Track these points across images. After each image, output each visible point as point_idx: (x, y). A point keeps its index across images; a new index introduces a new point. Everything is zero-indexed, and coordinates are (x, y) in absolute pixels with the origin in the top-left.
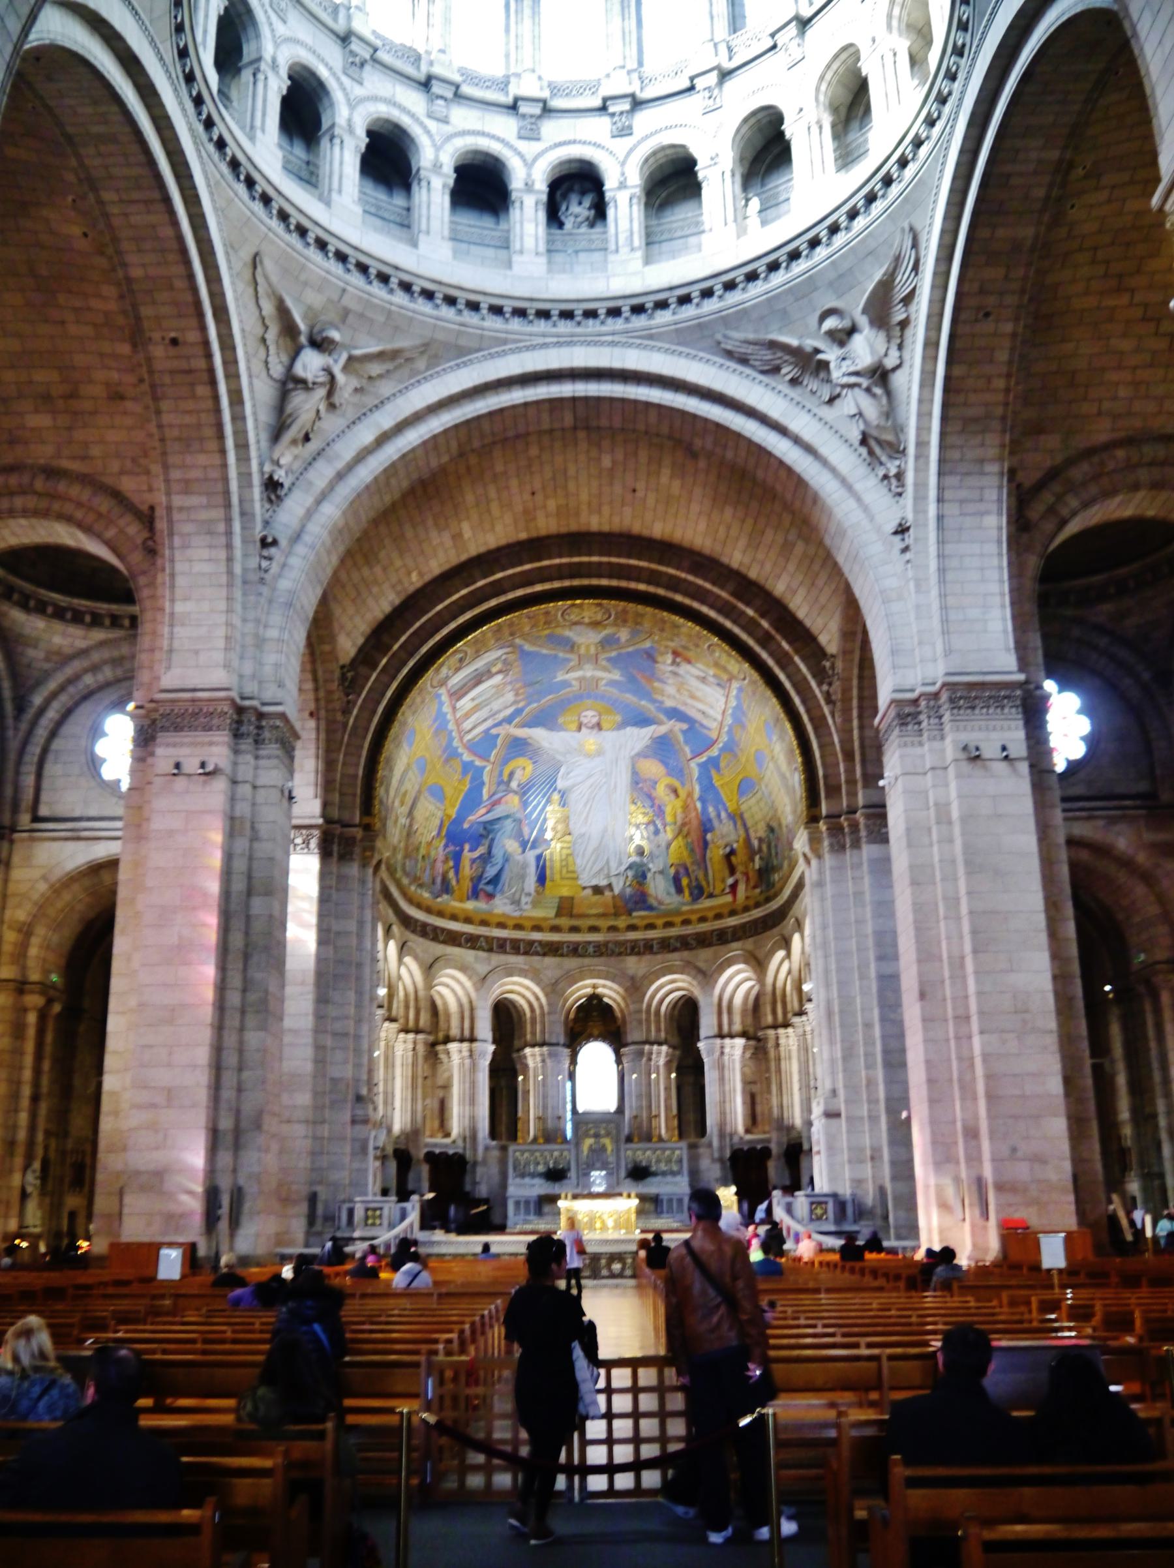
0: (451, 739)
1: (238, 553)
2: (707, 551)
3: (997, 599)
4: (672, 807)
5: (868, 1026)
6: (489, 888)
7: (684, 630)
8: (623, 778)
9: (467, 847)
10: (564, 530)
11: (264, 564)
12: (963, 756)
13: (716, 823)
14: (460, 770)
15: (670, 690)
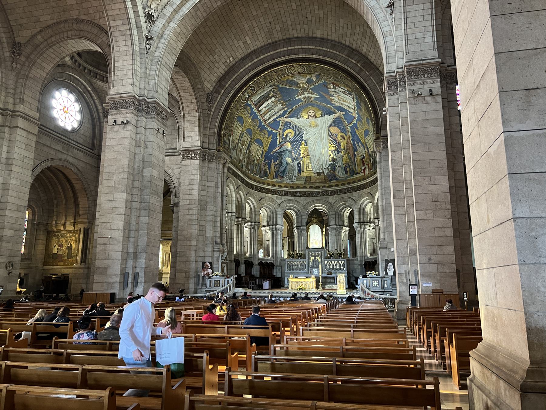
0: (261, 123)
1: (137, 42)
2: (337, 39)
4: (343, 143)
6: (281, 175)
7: (331, 72)
8: (326, 135)
9: (273, 161)
10: (284, 37)
11: (148, 47)
12: (411, 95)
13: (358, 147)
14: (267, 134)
15: (336, 99)
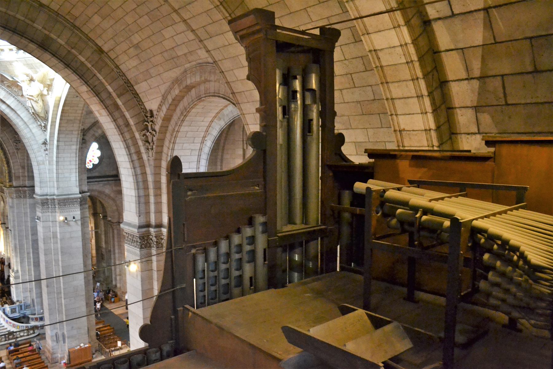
3: (74, 170)
5: (28, 253)
